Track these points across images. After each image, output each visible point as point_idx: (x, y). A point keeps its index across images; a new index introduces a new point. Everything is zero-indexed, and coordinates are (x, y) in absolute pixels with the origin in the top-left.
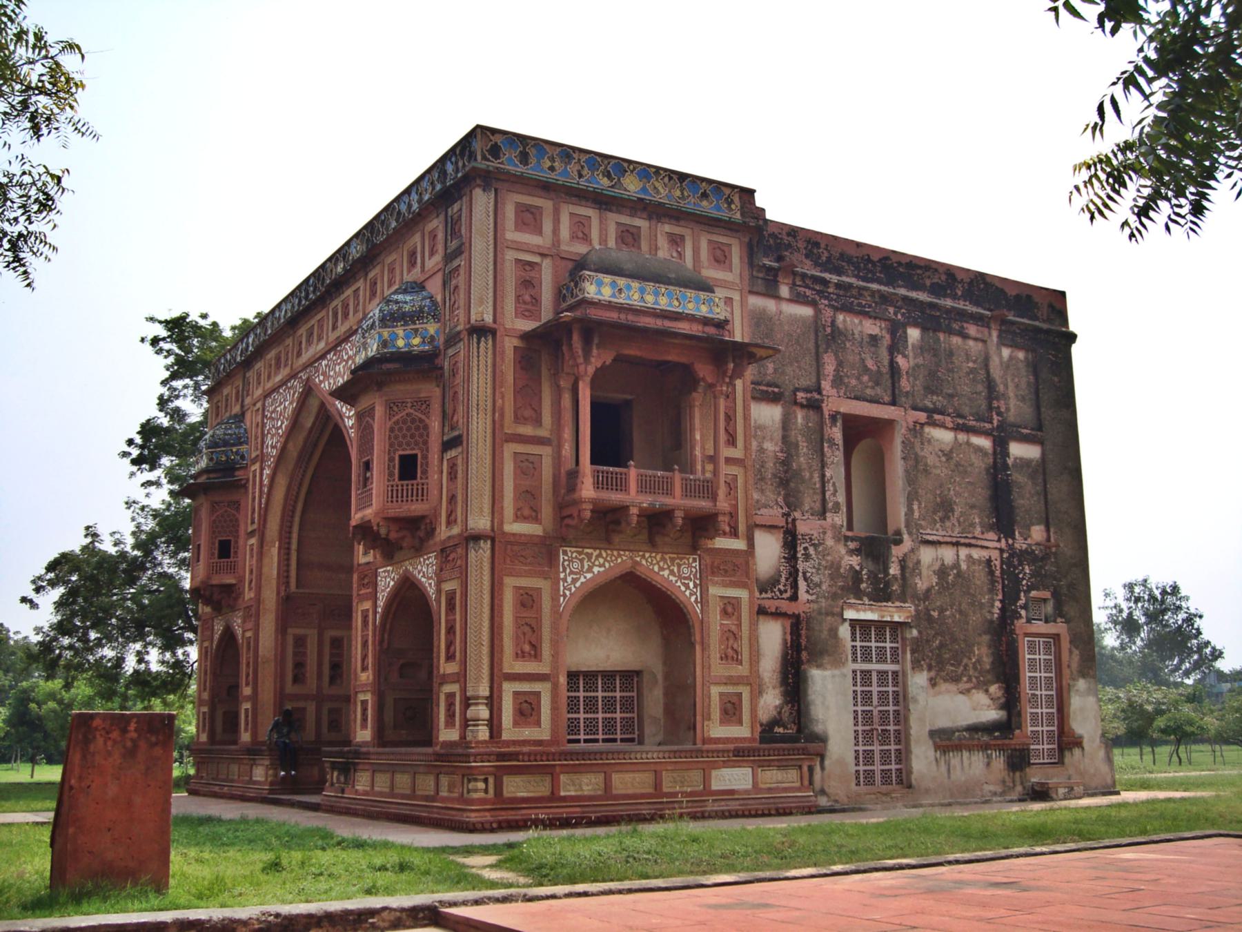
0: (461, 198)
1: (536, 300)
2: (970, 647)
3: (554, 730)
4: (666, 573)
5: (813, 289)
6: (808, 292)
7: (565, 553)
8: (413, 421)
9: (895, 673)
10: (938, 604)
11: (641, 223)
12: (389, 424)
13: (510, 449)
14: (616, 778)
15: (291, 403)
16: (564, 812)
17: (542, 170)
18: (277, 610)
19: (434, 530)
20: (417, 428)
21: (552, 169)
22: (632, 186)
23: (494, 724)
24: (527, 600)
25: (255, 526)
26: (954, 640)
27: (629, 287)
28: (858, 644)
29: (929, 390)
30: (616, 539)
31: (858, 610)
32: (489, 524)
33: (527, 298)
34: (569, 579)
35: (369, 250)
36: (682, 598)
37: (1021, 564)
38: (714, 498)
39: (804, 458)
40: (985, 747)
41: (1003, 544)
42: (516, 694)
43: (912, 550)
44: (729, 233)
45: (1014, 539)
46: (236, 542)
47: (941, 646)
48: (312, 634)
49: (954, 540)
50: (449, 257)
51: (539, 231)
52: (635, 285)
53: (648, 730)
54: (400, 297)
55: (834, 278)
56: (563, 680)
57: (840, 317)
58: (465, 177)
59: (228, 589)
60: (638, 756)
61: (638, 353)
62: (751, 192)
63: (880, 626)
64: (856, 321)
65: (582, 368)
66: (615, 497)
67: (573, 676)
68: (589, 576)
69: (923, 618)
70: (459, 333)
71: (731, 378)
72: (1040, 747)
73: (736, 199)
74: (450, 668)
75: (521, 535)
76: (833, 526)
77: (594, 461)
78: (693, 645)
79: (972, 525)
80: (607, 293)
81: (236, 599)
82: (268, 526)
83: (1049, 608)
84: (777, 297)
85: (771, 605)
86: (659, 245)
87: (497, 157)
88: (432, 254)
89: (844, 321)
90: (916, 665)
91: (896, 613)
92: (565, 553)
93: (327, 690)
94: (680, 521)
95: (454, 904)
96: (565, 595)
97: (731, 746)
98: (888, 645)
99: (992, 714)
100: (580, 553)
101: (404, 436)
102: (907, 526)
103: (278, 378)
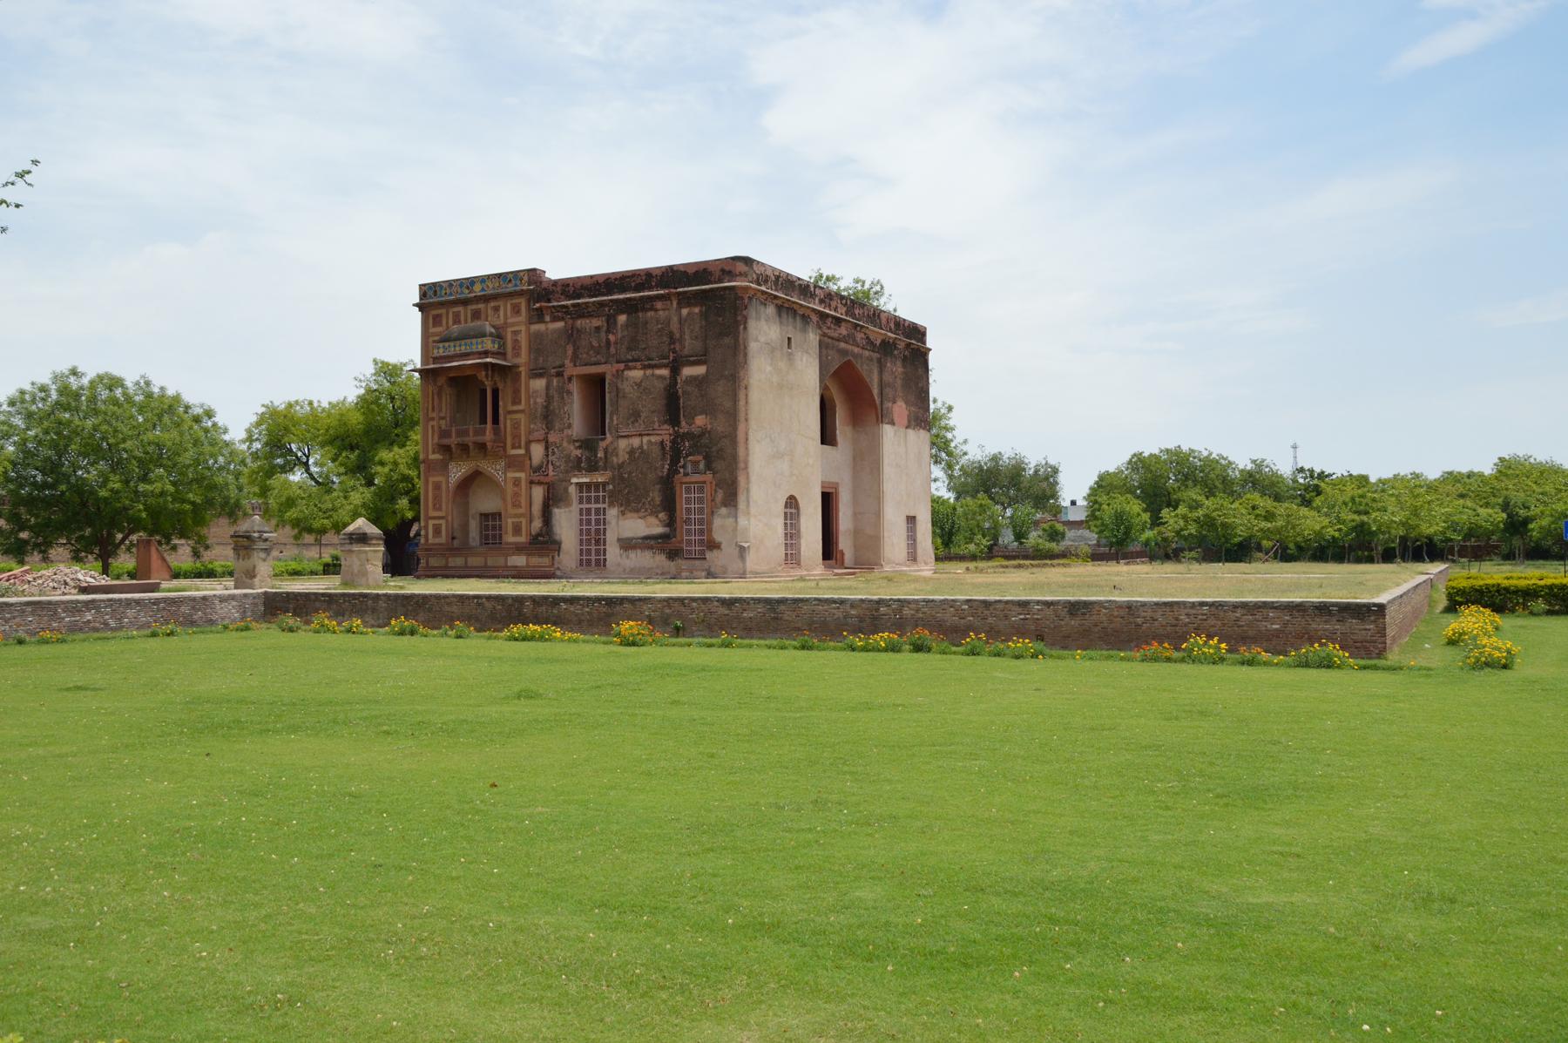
11: (481, 306)
24: (437, 487)
29: (629, 349)
40: (651, 548)
63: (588, 485)
83: (702, 466)
85: (536, 479)
90: (611, 504)
91: (600, 478)
99: (659, 530)
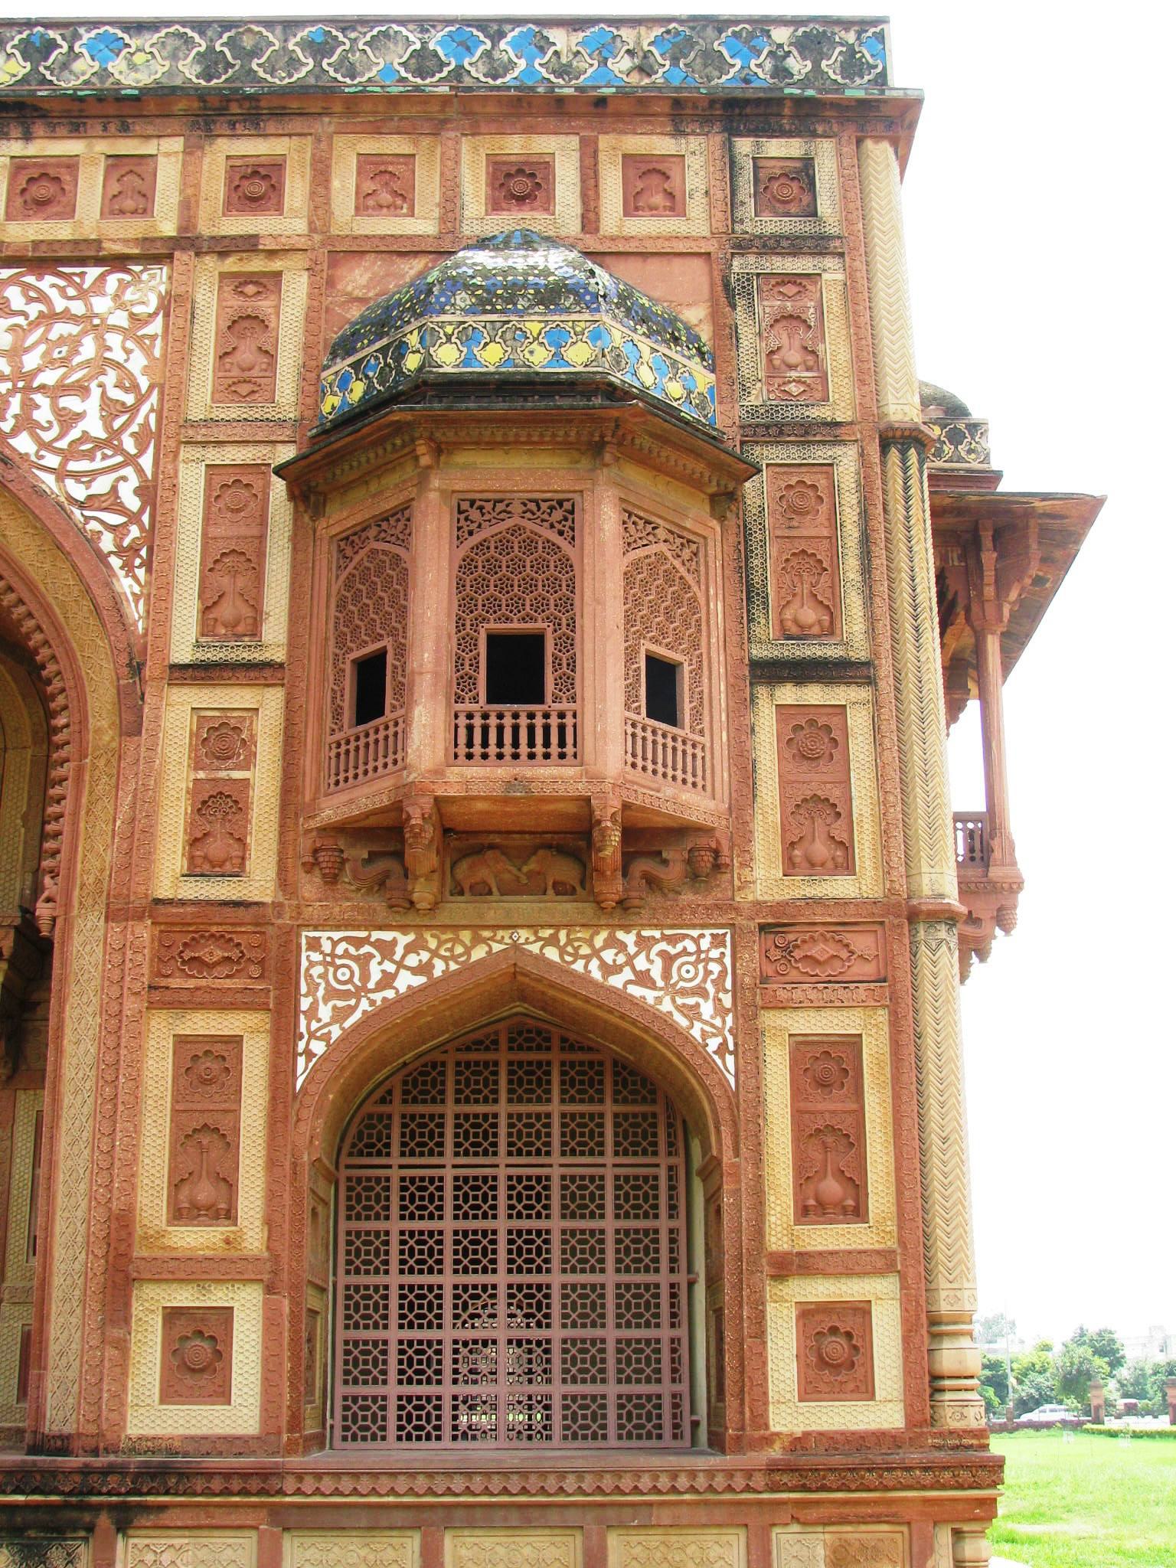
60: (570, 1483)
92: (314, 945)
100: (358, 943)
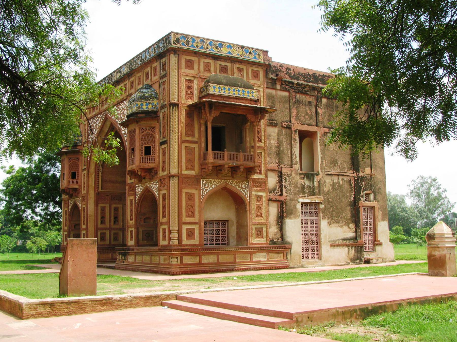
0: (165, 56)
1: (192, 93)
2: (343, 211)
3: (200, 241)
4: (237, 187)
5: (288, 86)
6: (287, 87)
7: (203, 181)
8: (149, 135)
9: (316, 220)
10: (332, 196)
12: (141, 136)
13: (184, 145)
14: (221, 257)
15: (99, 123)
16: (203, 268)
17: (194, 47)
18: (95, 196)
19: (157, 173)
20: (151, 137)
21: (197, 46)
22: (224, 52)
23: (180, 239)
24: (190, 197)
25: (86, 167)
26: (337, 209)
27: (224, 89)
28: (303, 210)
30: (220, 176)
31: (303, 199)
32: (177, 171)
33: (189, 92)
34: (204, 190)
35: (130, 71)
36: (243, 195)
37: (361, 181)
38: (254, 161)
39: (285, 146)
40: (347, 246)
41: (355, 175)
42: (187, 229)
43: (323, 177)
44: (259, 67)
45: (359, 173)
46: (78, 173)
47: (333, 210)
48: (107, 206)
49: (338, 173)
50: (161, 78)
51: (193, 69)
52: (227, 88)
53: (231, 240)
54: (144, 90)
55: (296, 82)
56: (202, 224)
57: (298, 95)
58: (168, 50)
59: (75, 190)
61: (228, 112)
62: (267, 52)
63: (311, 204)
64: (304, 96)
65: (209, 117)
66: (220, 162)
67: (205, 222)
68: (211, 188)
69: (327, 201)
70: (166, 104)
71: (260, 120)
72: (367, 245)
73: (262, 55)
74: (164, 220)
75: (188, 175)
76: (295, 169)
77: (212, 150)
78: (246, 211)
79: (344, 168)
80: (217, 92)
81: (78, 193)
82: (91, 167)
84: (276, 89)
85: (273, 197)
86: (235, 72)
87: (178, 43)
88: (155, 75)
89: (300, 97)
90: (324, 218)
93: (113, 226)
94: (242, 169)
95: (181, 293)
96: (203, 195)
97: (259, 246)
98: (314, 210)
99: (351, 234)
100: (208, 181)
101: (146, 140)
102: (321, 169)
103: (94, 113)
